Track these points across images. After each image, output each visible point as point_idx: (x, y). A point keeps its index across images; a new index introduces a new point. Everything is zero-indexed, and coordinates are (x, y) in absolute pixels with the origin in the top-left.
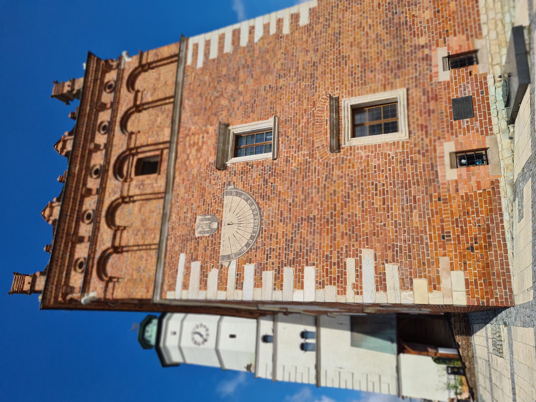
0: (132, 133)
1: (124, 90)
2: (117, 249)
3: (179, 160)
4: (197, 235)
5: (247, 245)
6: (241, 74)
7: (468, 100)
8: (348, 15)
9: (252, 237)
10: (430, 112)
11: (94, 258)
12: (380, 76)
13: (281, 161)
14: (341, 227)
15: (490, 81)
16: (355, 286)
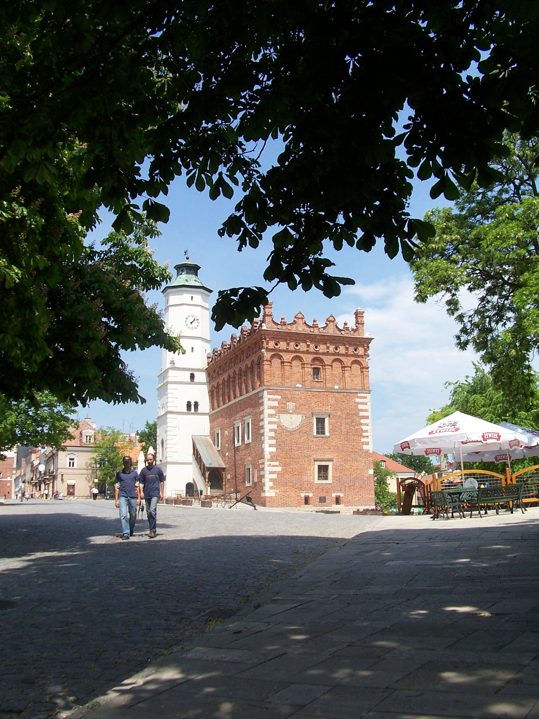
0: (332, 366)
1: (353, 359)
2: (283, 363)
3: (317, 393)
4: (287, 403)
5: (283, 425)
6: (350, 420)
7: (325, 502)
8: (363, 464)
9: (286, 427)
10: (323, 490)
11: (280, 352)
12: (338, 475)
13: (313, 439)
14: (288, 460)
15: (329, 508)
16: (270, 464)
